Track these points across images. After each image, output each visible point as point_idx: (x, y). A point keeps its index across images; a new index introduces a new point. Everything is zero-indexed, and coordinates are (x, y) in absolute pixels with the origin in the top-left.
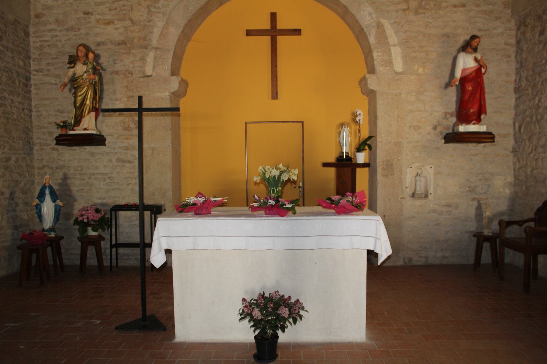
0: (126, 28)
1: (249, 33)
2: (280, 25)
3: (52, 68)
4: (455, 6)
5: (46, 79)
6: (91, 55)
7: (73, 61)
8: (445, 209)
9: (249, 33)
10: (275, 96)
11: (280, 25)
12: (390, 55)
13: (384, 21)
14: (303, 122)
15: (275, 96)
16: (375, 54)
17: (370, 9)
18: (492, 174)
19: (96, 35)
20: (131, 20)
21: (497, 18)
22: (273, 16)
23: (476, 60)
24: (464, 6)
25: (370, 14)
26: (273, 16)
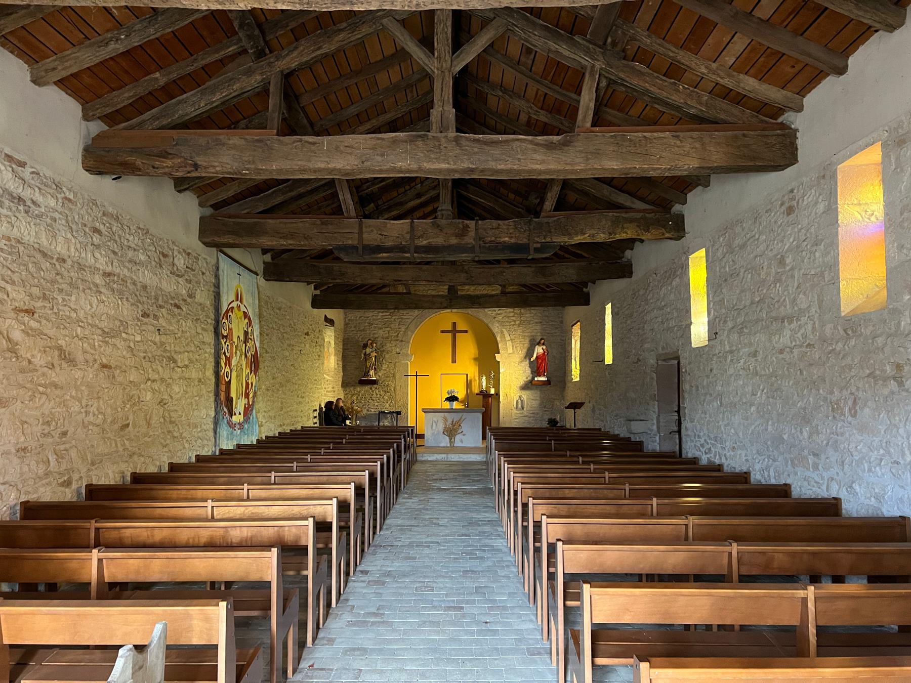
0: (389, 331)
1: (443, 332)
2: (458, 328)
3: (353, 348)
4: (536, 323)
5: (350, 353)
6: (375, 345)
7: (365, 346)
8: (532, 415)
9: (443, 332)
10: (454, 361)
11: (458, 328)
12: (506, 345)
13: (504, 330)
14: (467, 375)
15: (454, 361)
16: (500, 346)
17: (498, 325)
18: (554, 399)
19: (374, 334)
20: (391, 328)
21: (557, 328)
22: (454, 324)
23: (543, 349)
24: (541, 322)
25: (498, 327)
26: (454, 324)
